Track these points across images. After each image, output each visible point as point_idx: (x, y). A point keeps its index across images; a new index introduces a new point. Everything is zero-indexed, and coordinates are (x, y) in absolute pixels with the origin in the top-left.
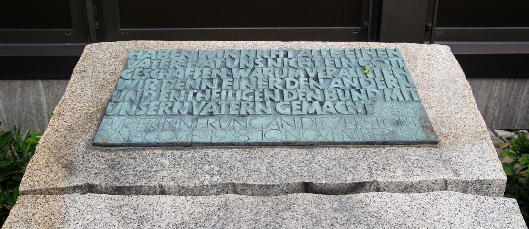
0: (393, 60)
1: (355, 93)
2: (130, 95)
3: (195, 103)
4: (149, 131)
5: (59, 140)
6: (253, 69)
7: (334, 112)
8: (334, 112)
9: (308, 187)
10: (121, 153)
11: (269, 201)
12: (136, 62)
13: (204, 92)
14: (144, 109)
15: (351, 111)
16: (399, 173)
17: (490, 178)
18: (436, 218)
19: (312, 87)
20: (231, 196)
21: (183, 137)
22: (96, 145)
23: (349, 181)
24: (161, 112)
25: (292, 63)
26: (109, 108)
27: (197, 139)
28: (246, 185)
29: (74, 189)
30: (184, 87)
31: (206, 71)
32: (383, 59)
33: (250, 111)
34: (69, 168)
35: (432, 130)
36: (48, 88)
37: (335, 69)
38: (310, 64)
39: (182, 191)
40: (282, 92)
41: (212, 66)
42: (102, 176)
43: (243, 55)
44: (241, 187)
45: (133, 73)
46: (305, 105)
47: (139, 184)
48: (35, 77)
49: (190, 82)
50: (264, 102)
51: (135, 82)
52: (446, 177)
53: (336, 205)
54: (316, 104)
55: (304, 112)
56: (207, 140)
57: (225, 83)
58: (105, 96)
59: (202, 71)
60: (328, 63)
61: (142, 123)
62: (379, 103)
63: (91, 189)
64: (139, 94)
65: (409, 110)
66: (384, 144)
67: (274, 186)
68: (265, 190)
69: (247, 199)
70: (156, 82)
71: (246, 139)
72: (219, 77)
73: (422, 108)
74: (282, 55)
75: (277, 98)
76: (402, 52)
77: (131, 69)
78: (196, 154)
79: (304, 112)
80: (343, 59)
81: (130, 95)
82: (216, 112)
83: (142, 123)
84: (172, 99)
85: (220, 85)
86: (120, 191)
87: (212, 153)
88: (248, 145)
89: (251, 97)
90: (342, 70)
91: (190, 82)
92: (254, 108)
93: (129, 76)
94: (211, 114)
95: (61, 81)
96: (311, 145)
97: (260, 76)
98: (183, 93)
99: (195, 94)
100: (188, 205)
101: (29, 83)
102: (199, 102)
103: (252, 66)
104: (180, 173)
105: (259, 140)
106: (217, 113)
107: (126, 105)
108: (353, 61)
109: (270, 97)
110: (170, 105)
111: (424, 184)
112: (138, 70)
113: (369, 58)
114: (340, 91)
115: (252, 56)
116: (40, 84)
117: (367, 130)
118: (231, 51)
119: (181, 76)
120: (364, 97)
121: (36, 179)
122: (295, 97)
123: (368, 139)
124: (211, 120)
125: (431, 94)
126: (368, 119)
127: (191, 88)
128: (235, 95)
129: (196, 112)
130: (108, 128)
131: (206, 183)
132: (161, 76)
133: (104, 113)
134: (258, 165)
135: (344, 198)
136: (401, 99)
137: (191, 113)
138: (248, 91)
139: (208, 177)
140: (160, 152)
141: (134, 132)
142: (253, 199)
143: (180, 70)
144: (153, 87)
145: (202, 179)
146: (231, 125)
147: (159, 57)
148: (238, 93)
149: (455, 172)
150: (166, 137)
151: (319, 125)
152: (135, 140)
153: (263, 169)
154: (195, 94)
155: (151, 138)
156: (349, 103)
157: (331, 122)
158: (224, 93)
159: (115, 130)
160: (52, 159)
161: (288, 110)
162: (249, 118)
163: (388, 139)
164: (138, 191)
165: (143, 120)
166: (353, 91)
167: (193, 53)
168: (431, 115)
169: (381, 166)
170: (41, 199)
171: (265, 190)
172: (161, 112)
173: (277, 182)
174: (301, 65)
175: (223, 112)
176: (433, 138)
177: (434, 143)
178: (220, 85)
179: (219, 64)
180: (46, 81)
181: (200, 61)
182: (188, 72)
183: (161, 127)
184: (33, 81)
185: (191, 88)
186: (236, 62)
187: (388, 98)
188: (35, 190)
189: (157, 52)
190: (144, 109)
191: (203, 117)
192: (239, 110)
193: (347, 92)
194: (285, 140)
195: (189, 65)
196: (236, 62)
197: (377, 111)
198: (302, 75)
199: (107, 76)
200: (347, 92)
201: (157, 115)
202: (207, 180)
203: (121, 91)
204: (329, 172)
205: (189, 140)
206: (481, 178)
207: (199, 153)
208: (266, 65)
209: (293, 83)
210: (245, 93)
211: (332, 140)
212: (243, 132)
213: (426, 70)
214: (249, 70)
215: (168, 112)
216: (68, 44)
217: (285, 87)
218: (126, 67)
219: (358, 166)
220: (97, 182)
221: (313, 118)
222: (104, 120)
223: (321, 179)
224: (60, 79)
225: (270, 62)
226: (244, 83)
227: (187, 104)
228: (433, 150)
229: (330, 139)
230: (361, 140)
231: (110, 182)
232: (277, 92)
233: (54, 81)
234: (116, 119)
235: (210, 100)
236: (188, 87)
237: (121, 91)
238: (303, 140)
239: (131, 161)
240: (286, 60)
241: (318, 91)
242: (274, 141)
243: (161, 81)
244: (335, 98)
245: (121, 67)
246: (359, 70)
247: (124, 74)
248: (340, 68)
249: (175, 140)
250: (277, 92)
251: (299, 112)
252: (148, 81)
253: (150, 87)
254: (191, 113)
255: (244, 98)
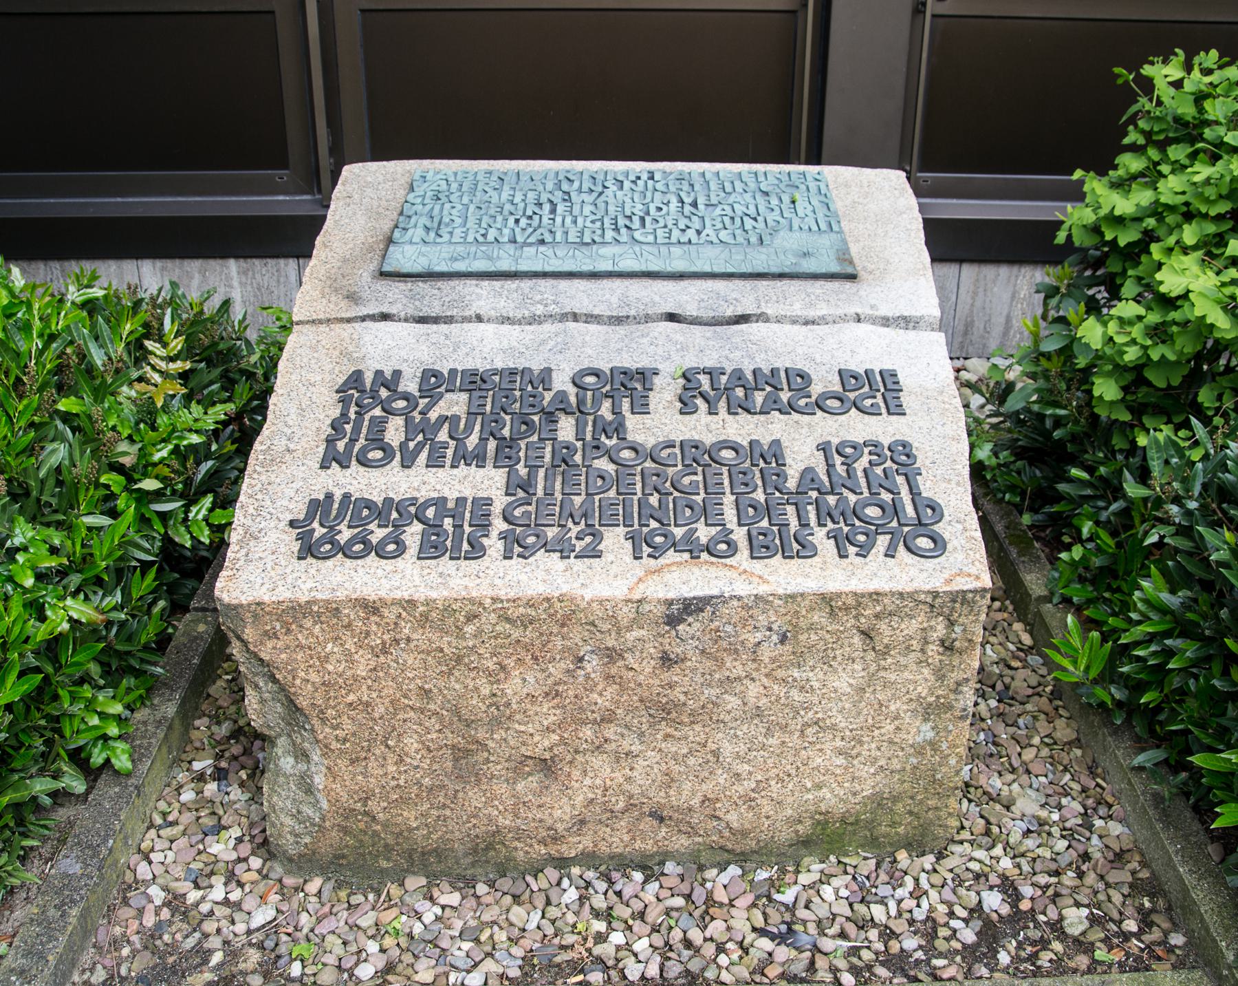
0: (812, 185)
1: (749, 223)
2: (424, 220)
3: (517, 230)
4: (456, 260)
5: (333, 271)
6: (601, 194)
7: (715, 240)
8: (715, 240)
9: (672, 317)
10: (420, 284)
11: (621, 330)
12: (426, 185)
13: (530, 218)
14: (446, 237)
15: (740, 239)
16: (797, 306)
17: (918, 314)
18: (835, 346)
19: (687, 212)
20: (571, 325)
21: (505, 265)
22: (383, 275)
23: (729, 313)
24: (470, 239)
25: (659, 186)
26: (397, 234)
27: (523, 267)
28: (592, 316)
29: (363, 319)
30: (501, 213)
31: (531, 196)
32: (797, 184)
33: (597, 239)
34: (353, 298)
35: (851, 262)
36: (245, 273)
37: (723, 195)
38: (686, 187)
39: (506, 320)
40: (642, 220)
41: (541, 188)
42: (400, 306)
43: (585, 177)
44: (584, 318)
45: (424, 197)
46: (676, 234)
47: (449, 314)
48: (224, 255)
49: (508, 207)
50: (617, 230)
51: (428, 207)
52: (859, 311)
53: (708, 335)
54: (691, 234)
55: (674, 239)
56: (538, 267)
57: (560, 208)
58: (387, 225)
59: (525, 195)
60: (713, 186)
61: (446, 251)
62: (782, 233)
63: (385, 317)
64: (436, 220)
65: (826, 242)
66: (781, 276)
67: (628, 317)
68: (618, 320)
69: (593, 328)
70: (459, 207)
71: (591, 268)
72: (551, 201)
73: (844, 242)
74: (645, 176)
75: (636, 223)
76: (830, 179)
77: (419, 191)
78: (522, 285)
79: (674, 239)
80: (738, 184)
81: (424, 220)
82: (548, 238)
83: (446, 251)
84: (484, 225)
85: (553, 211)
86: (422, 320)
87: (542, 283)
88: (594, 275)
89: (598, 224)
90: (733, 195)
91: (508, 207)
92: (603, 236)
93: (419, 200)
94: (542, 242)
95: (269, 260)
96: (681, 276)
97: (611, 200)
98: (499, 218)
99: (517, 221)
100: (515, 333)
101: (214, 264)
102: (524, 230)
103: (600, 189)
104: (502, 303)
105: (610, 268)
106: (550, 240)
107: (420, 232)
108: (752, 185)
109: (624, 225)
110: (483, 232)
111: (830, 319)
112: (430, 194)
113: (776, 182)
114: (727, 220)
115: (600, 177)
116: (232, 265)
117: (760, 260)
118: (568, 171)
119: (495, 200)
120: (761, 225)
121: (312, 309)
122: (661, 224)
123: (761, 270)
124: (542, 249)
125: (861, 227)
126: (764, 250)
127: (512, 214)
128: (575, 222)
129: (520, 239)
130: (399, 256)
131: (538, 313)
132: (465, 200)
133: (390, 241)
134: (608, 296)
135: (718, 328)
136: (815, 228)
137: (513, 241)
138: (594, 217)
139: (541, 307)
140: (474, 282)
141: (435, 261)
142: (599, 327)
143: (495, 194)
144: (454, 212)
145: (533, 309)
146: (571, 253)
147: (459, 178)
148: (580, 220)
149: (872, 307)
150: (480, 265)
151: (694, 254)
152: (438, 269)
153: (614, 300)
154: (517, 221)
155: (460, 266)
156: (738, 232)
157: (709, 252)
158: (559, 220)
159: (405, 257)
160: (327, 290)
161: (651, 238)
162: (595, 247)
163: (787, 270)
164: (449, 320)
165: (445, 248)
166: (745, 218)
167: (510, 174)
168: (854, 250)
169: (774, 298)
170: (323, 328)
171: (618, 320)
172: (470, 239)
173: (632, 313)
174: (672, 188)
175: (558, 239)
176: (850, 270)
177: (852, 277)
178: (553, 211)
179: (550, 186)
180: (242, 260)
181: (521, 184)
182: (505, 195)
183: (472, 256)
184: (220, 261)
185: (512, 214)
186: (576, 184)
187: (795, 227)
188: (313, 321)
189: (456, 174)
190: (446, 237)
191: (531, 244)
192: (582, 237)
193: (738, 220)
194: (644, 268)
195: (506, 187)
196: (576, 184)
197: (778, 241)
198: (674, 200)
199: (383, 203)
200: (738, 220)
201: (465, 242)
202: (539, 310)
203: (409, 217)
204: (702, 304)
205: (513, 269)
206: (906, 314)
207: (526, 284)
208: (621, 188)
209: (660, 209)
210: (589, 219)
211: (709, 270)
212: (588, 261)
213: (861, 200)
214: (595, 195)
215: (481, 239)
216: (281, 198)
217: (648, 213)
218: (412, 189)
219: (743, 297)
220: (393, 310)
221: (686, 248)
222: (391, 248)
223: (691, 310)
224: (266, 257)
225: (627, 185)
226: (587, 209)
227: (506, 231)
228: (848, 285)
229: (707, 269)
230: (750, 271)
231: (410, 311)
232: (636, 219)
233: (257, 262)
234: (407, 247)
235: (539, 226)
236: (506, 212)
237: (409, 217)
238: (669, 269)
239: (436, 292)
240: (650, 183)
241: (695, 218)
242: (629, 270)
243: (467, 207)
244: (720, 226)
245: (403, 192)
246: (758, 195)
247: (411, 197)
248: (730, 193)
249: (493, 269)
250: (636, 219)
251: (667, 241)
252: (448, 206)
253: (453, 213)
254: (513, 241)
255: (588, 224)
